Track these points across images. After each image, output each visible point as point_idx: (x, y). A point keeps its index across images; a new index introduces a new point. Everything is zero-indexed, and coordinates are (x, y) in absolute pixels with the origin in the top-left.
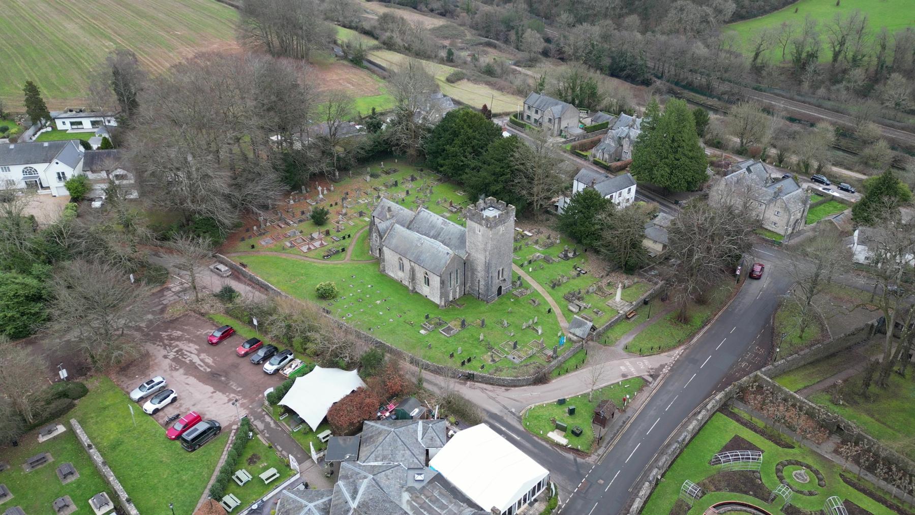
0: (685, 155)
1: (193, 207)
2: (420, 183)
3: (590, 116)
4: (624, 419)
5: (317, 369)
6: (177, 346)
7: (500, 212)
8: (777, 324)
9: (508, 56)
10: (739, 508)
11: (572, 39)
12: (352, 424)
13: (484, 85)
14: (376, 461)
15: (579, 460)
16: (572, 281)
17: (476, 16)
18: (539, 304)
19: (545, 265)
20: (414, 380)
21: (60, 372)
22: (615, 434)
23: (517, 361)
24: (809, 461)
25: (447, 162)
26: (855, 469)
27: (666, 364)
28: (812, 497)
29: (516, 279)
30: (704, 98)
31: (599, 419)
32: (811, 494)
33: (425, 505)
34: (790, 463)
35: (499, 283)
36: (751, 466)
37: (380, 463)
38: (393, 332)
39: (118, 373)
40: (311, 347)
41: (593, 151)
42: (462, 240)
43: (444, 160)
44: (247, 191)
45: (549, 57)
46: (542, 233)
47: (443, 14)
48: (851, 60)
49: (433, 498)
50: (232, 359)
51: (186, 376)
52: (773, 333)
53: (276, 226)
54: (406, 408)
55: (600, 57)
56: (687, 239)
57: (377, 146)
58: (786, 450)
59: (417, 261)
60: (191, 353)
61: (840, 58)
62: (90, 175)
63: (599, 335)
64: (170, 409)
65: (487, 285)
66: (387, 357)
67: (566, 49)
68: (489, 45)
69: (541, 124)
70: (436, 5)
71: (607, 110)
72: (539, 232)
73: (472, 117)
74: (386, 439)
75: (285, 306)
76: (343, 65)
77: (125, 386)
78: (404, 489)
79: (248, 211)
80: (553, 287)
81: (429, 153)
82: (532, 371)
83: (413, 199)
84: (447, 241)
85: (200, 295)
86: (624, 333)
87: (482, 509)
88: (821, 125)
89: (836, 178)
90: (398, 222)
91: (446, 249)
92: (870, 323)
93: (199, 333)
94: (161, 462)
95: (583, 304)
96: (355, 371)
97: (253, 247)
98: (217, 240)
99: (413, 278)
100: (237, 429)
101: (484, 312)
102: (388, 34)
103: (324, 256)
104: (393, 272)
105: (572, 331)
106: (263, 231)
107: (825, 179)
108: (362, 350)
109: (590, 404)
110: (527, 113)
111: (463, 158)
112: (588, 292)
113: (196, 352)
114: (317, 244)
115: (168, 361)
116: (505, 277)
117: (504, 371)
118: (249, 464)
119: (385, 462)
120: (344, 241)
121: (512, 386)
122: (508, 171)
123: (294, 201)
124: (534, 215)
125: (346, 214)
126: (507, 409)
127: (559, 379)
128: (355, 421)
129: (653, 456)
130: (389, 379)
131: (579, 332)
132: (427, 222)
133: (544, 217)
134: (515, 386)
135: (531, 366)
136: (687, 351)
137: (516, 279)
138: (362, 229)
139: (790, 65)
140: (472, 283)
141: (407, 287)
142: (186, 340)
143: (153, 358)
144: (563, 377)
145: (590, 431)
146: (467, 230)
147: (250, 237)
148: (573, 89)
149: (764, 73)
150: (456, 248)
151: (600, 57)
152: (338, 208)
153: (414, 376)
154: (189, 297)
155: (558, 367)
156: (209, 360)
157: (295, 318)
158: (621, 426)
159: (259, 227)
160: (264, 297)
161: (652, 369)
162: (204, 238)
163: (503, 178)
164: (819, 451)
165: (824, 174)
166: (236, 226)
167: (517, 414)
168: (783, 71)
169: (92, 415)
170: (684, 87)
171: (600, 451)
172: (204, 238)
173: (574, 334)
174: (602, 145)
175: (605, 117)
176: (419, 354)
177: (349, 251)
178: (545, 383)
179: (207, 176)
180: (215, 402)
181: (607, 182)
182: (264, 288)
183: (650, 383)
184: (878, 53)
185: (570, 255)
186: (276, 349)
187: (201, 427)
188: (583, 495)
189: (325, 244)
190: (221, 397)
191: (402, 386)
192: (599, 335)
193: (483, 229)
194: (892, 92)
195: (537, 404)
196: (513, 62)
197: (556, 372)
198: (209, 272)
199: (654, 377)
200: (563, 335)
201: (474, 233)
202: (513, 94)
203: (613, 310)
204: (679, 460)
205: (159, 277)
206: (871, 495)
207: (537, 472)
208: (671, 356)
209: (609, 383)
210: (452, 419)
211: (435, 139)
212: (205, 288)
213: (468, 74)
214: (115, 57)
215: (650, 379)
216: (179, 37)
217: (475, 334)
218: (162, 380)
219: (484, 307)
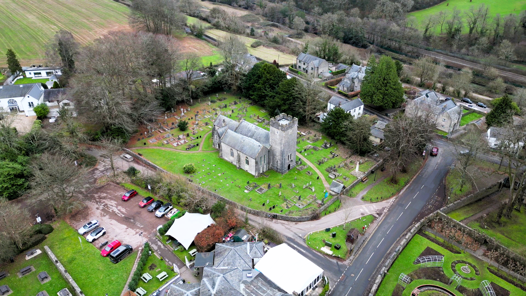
0: (391, 87)
1: (110, 121)
2: (240, 106)
3: (335, 66)
4: (364, 239)
5: (187, 214)
6: (104, 202)
7: (289, 122)
8: (447, 183)
9: (285, 32)
10: (432, 288)
11: (321, 22)
12: (209, 245)
13: (273, 49)
14: (224, 266)
15: (340, 263)
16: (330, 161)
17: (266, 9)
18: (312, 174)
19: (314, 152)
20: (243, 220)
21: (37, 219)
22: (359, 248)
23: (301, 207)
24: (470, 260)
25: (255, 93)
26: (496, 265)
27: (386, 207)
28: (473, 281)
29: (298, 160)
30: (397, 55)
31: (350, 239)
32: (472, 279)
33: (254, 291)
34: (459, 262)
35: (289, 162)
36: (437, 264)
37: (226, 268)
38: (229, 192)
39: (70, 218)
40: (183, 201)
41: (338, 86)
42: (267, 138)
43: (253, 92)
44: (141, 112)
45: (309, 32)
46: (311, 133)
47: (246, 8)
48: (480, 33)
49: (258, 287)
50: (137, 209)
51: (110, 220)
52: (445, 188)
53: (158, 132)
54: (239, 235)
55: (338, 32)
56: (396, 135)
57: (214, 84)
58: (456, 254)
59: (241, 150)
60: (112, 206)
61: (473, 31)
62: (48, 104)
63: (347, 191)
64: (102, 239)
65: (282, 164)
66: (227, 207)
67: (318, 28)
68: (273, 25)
69: (307, 71)
70: (242, 3)
71: (344, 62)
72: (309, 133)
73: (269, 67)
74: (230, 253)
75: (166, 177)
76: (191, 38)
77: (75, 226)
78: (241, 282)
79: (142, 123)
80: (319, 164)
81: (244, 88)
82: (310, 213)
83: (236, 115)
84: (258, 139)
85: (116, 173)
86: (361, 189)
87: (286, 293)
88: (464, 70)
89: (475, 99)
90: (229, 128)
91: (258, 143)
92: (499, 181)
93: (116, 194)
94: (99, 270)
95: (337, 174)
96: (209, 215)
97: (145, 144)
98: (124, 140)
99: (239, 160)
100: (142, 250)
101: (281, 179)
102: (216, 20)
103: (186, 149)
104: (227, 157)
105: (332, 189)
106: (150, 135)
107: (469, 100)
108: (212, 203)
109: (344, 231)
110: (299, 64)
111: (264, 91)
112: (339, 167)
113: (115, 206)
114: (182, 142)
115: (99, 211)
116: (292, 159)
117: (294, 213)
118: (150, 270)
119: (229, 267)
120: (197, 140)
121: (299, 222)
122: (291, 98)
123: (167, 117)
124: (306, 123)
125: (198, 124)
126: (296, 234)
127: (325, 217)
128: (211, 244)
129: (381, 259)
130: (229, 219)
131: (336, 190)
132: (246, 128)
133: (312, 124)
134: (301, 221)
135: (310, 210)
136: (397, 199)
137: (298, 160)
138: (208, 132)
139: (446, 35)
140: (273, 163)
141: (235, 166)
142: (109, 198)
143: (91, 209)
144: (328, 216)
145: (345, 246)
146: (270, 132)
147: (143, 138)
148: (324, 51)
149: (431, 40)
150: (264, 142)
151: (338, 32)
152: (193, 120)
153: (243, 217)
154: (110, 173)
155: (324, 210)
156: (123, 210)
157: (173, 184)
158: (362, 243)
159: (148, 132)
160: (153, 173)
161: (378, 210)
162: (118, 139)
163: (288, 102)
164: (475, 255)
165: (468, 97)
166: (136, 132)
167: (303, 237)
168: (441, 39)
169: (57, 243)
170: (386, 49)
171: (351, 258)
172: (118, 139)
173: (333, 191)
174: (343, 83)
175: (343, 66)
176: (245, 204)
177: (201, 145)
178: (318, 219)
179: (118, 103)
180: (128, 234)
181: (347, 104)
182: (154, 168)
183: (377, 218)
184: (495, 28)
185: (328, 146)
186: (162, 203)
187: (121, 249)
188: (343, 283)
189: (187, 141)
190: (131, 231)
191: (236, 223)
192: (347, 191)
193: (279, 131)
194: (503, 50)
195: (314, 232)
196: (288, 35)
197: (323, 213)
198: (121, 159)
199: (379, 214)
200: (327, 192)
201: (274, 134)
202: (289, 54)
203: (354, 177)
204: (396, 261)
205: (92, 162)
206: (506, 279)
207: (318, 271)
208: (388, 202)
209: (353, 219)
210: (266, 241)
211: (248, 80)
212: (118, 168)
213: (264, 43)
214: (59, 35)
215: (377, 216)
216: (95, 23)
217: (276, 192)
218: (96, 222)
219: (280, 177)
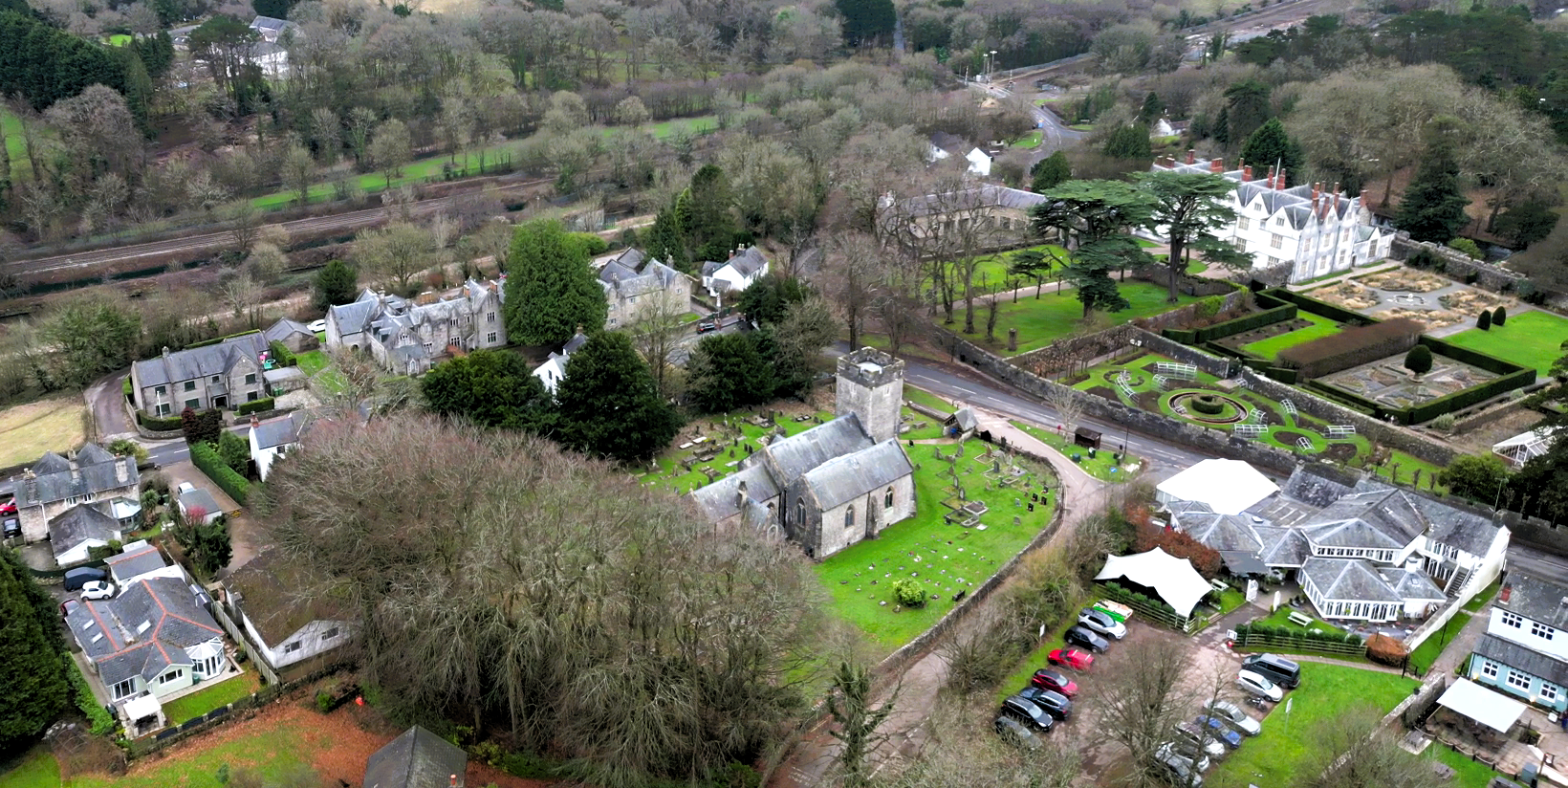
84: (838, 450)
132: (793, 454)
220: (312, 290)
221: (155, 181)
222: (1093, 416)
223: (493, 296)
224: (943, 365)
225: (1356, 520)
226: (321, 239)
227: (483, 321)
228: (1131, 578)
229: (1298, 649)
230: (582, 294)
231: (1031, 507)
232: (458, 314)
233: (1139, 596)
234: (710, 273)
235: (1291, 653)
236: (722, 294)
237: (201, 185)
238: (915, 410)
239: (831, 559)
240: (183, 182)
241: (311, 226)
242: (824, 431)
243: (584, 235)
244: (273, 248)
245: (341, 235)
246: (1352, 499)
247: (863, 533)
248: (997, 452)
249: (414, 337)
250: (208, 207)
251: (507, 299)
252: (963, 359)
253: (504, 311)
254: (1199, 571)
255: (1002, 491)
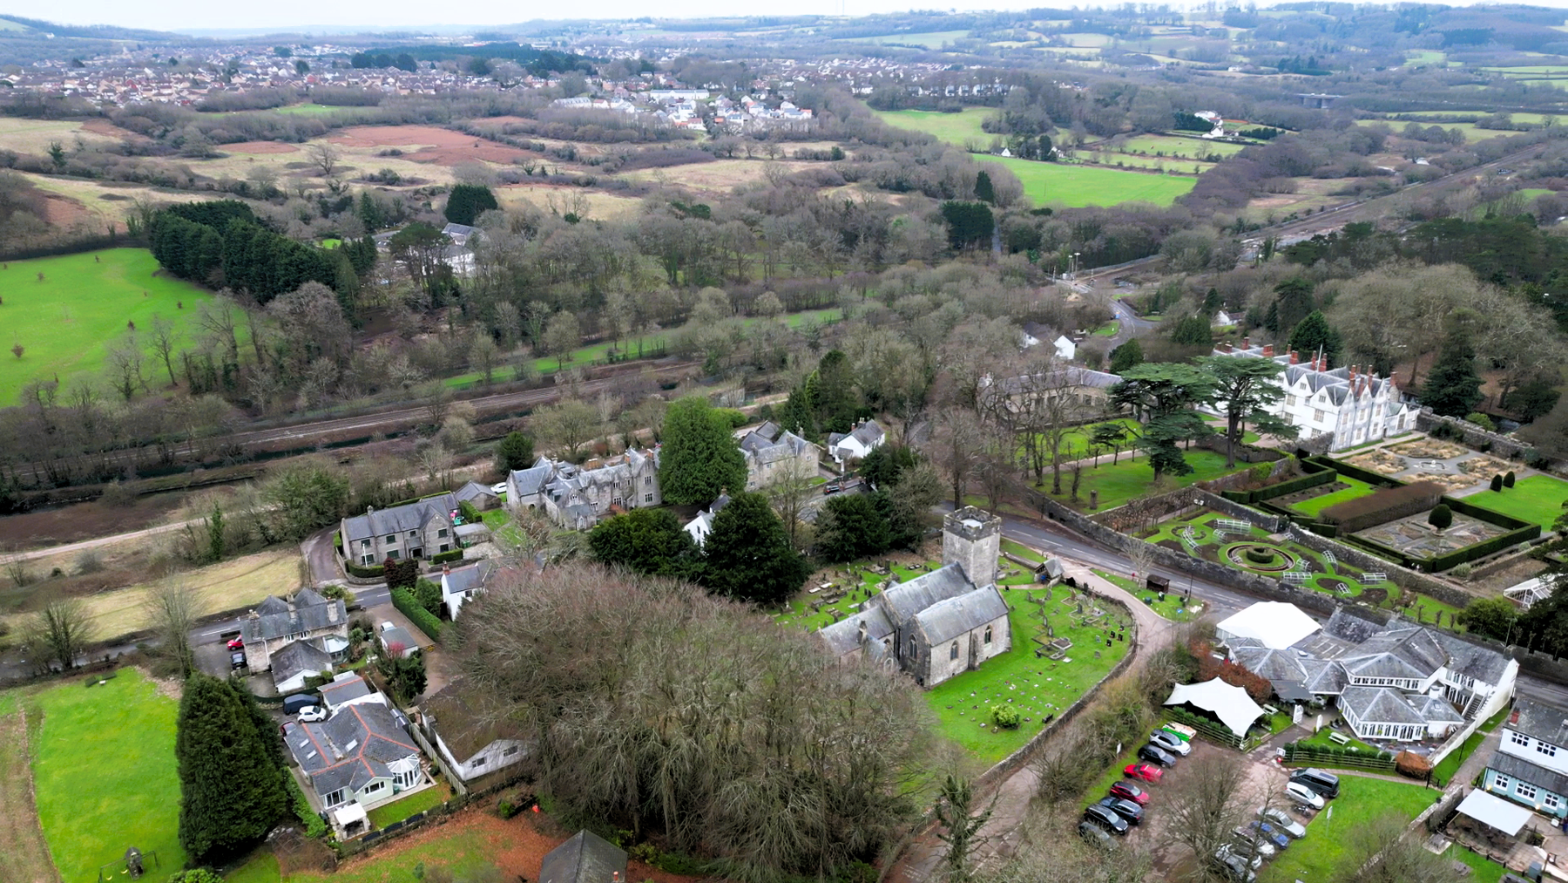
84: (944, 594)
132: (906, 598)
220: (495, 457)
221: (361, 364)
222: (1163, 565)
223: (650, 462)
224: (1034, 521)
225: (1387, 654)
226: (503, 414)
227: (641, 484)
228: (1195, 704)
229: (1337, 764)
230: (726, 461)
231: (1109, 643)
232: (620, 478)
233: (1202, 719)
234: (835, 443)
235: (1331, 767)
236: (845, 460)
237: (401, 368)
238: (1010, 560)
239: (938, 687)
240: (385, 365)
241: (495, 403)
242: (933, 578)
243: (727, 410)
244: (462, 422)
245: (520, 410)
246: (1383, 636)
247: (966, 665)
248: (1081, 596)
249: (582, 498)
250: (406, 387)
251: (661, 465)
252: (1051, 516)
253: (659, 474)
254: (1253, 697)
255: (1085, 629)
